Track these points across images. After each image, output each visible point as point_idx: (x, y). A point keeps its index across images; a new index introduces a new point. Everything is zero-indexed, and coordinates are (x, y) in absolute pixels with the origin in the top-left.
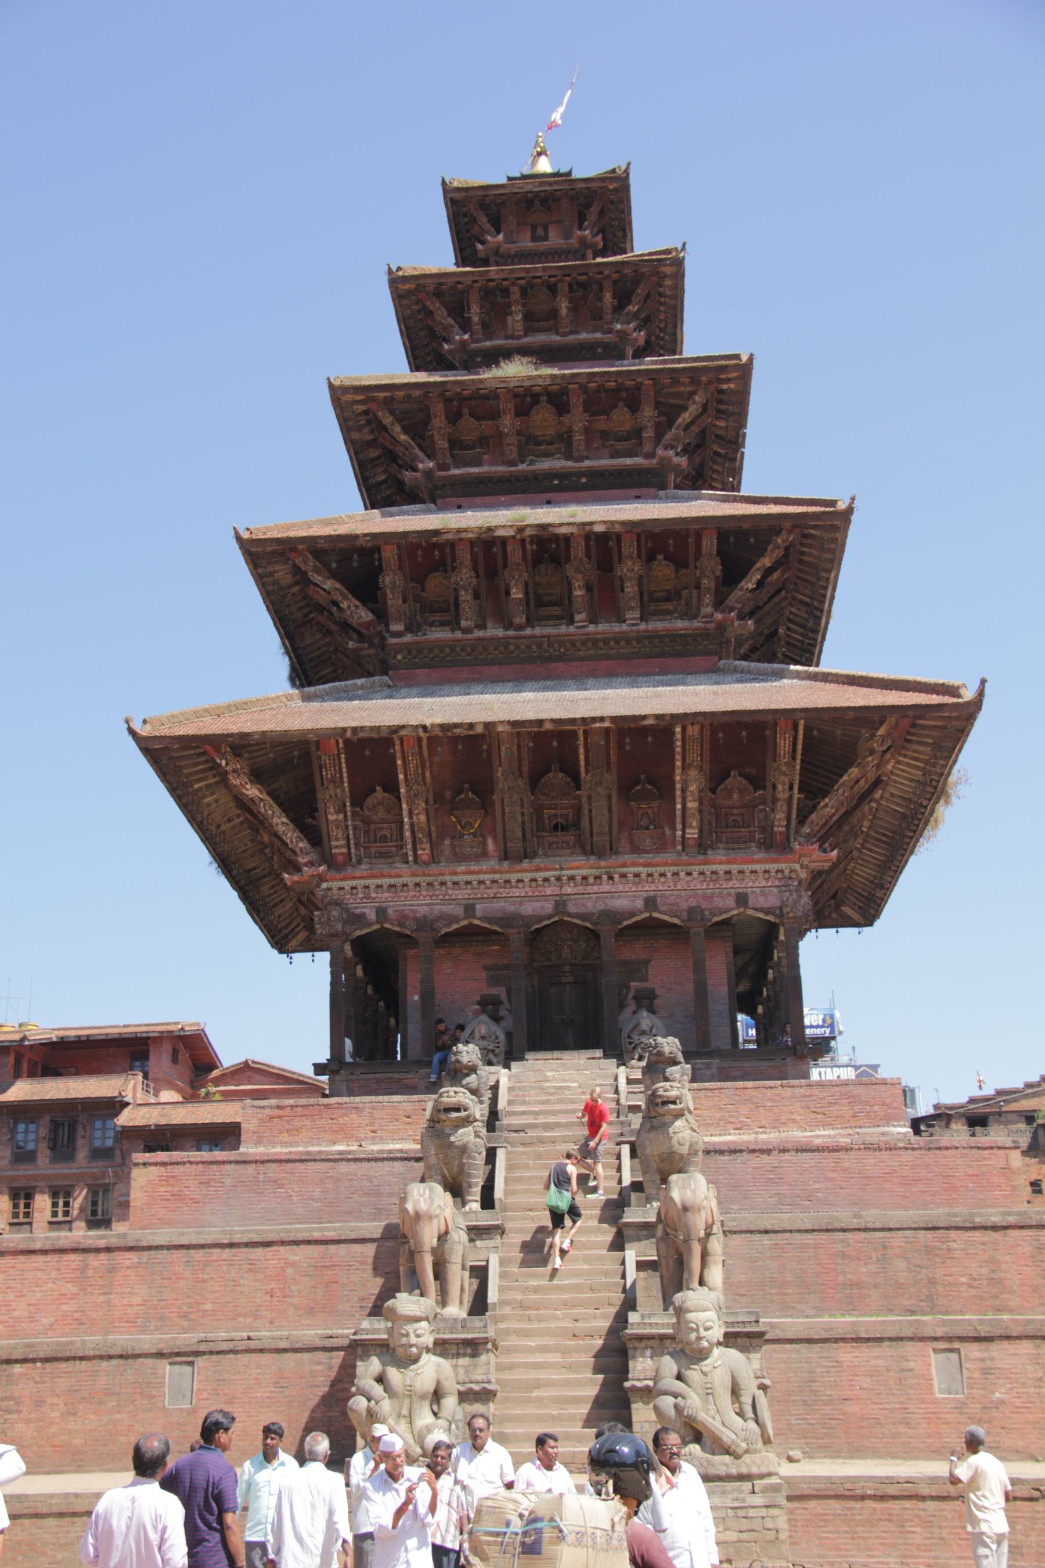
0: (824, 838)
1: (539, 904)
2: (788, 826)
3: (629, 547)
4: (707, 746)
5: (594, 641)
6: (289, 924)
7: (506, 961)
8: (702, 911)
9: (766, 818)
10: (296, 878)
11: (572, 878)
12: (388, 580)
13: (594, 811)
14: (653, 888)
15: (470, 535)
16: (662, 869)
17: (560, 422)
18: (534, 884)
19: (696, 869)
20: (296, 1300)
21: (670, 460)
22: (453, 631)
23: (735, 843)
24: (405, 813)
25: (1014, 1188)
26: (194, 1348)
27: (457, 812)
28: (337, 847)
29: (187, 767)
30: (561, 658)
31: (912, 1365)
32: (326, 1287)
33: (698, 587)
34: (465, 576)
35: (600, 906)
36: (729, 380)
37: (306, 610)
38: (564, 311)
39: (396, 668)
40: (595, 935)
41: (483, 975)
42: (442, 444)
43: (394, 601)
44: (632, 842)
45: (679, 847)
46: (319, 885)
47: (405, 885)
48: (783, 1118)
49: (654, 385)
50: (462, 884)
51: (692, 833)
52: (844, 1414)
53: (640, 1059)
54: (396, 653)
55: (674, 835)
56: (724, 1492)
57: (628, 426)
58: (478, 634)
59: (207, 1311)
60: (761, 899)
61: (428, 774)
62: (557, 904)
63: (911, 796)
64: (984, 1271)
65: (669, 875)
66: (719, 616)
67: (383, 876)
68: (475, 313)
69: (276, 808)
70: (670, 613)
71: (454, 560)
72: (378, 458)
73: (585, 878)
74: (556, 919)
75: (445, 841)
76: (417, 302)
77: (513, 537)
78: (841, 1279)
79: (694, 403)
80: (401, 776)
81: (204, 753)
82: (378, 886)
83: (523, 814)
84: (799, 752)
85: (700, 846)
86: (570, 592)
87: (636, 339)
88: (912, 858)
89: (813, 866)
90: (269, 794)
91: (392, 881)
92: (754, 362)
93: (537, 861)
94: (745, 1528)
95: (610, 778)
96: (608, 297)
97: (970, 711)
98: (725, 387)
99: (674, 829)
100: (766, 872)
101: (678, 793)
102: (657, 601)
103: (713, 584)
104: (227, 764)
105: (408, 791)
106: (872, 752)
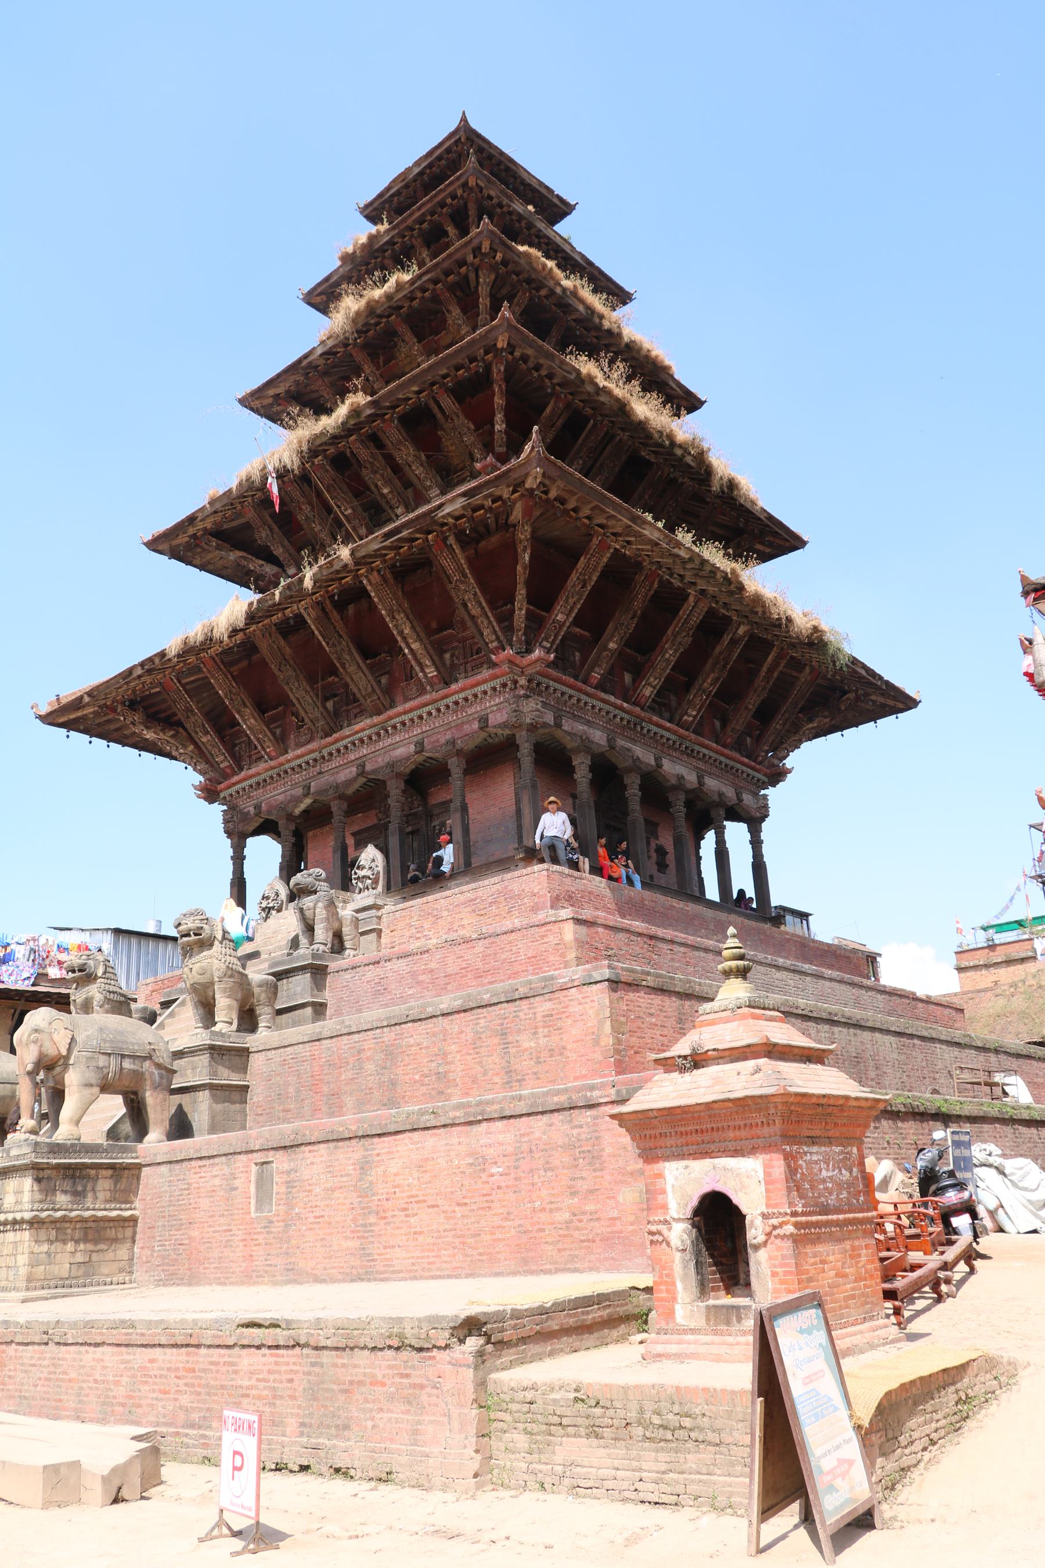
1: (347, 771)
2: (498, 638)
3: (393, 433)
12: (264, 536)
14: (419, 731)
19: (441, 705)
31: (237, 1183)
43: (278, 551)
44: (404, 695)
45: (428, 688)
47: (265, 780)
51: (431, 672)
52: (190, 1238)
60: (498, 716)
64: (434, 1064)
74: (362, 780)
78: (325, 1089)
82: (251, 786)
84: (465, 566)
89: (530, 671)
96: (451, 230)
100: (494, 689)
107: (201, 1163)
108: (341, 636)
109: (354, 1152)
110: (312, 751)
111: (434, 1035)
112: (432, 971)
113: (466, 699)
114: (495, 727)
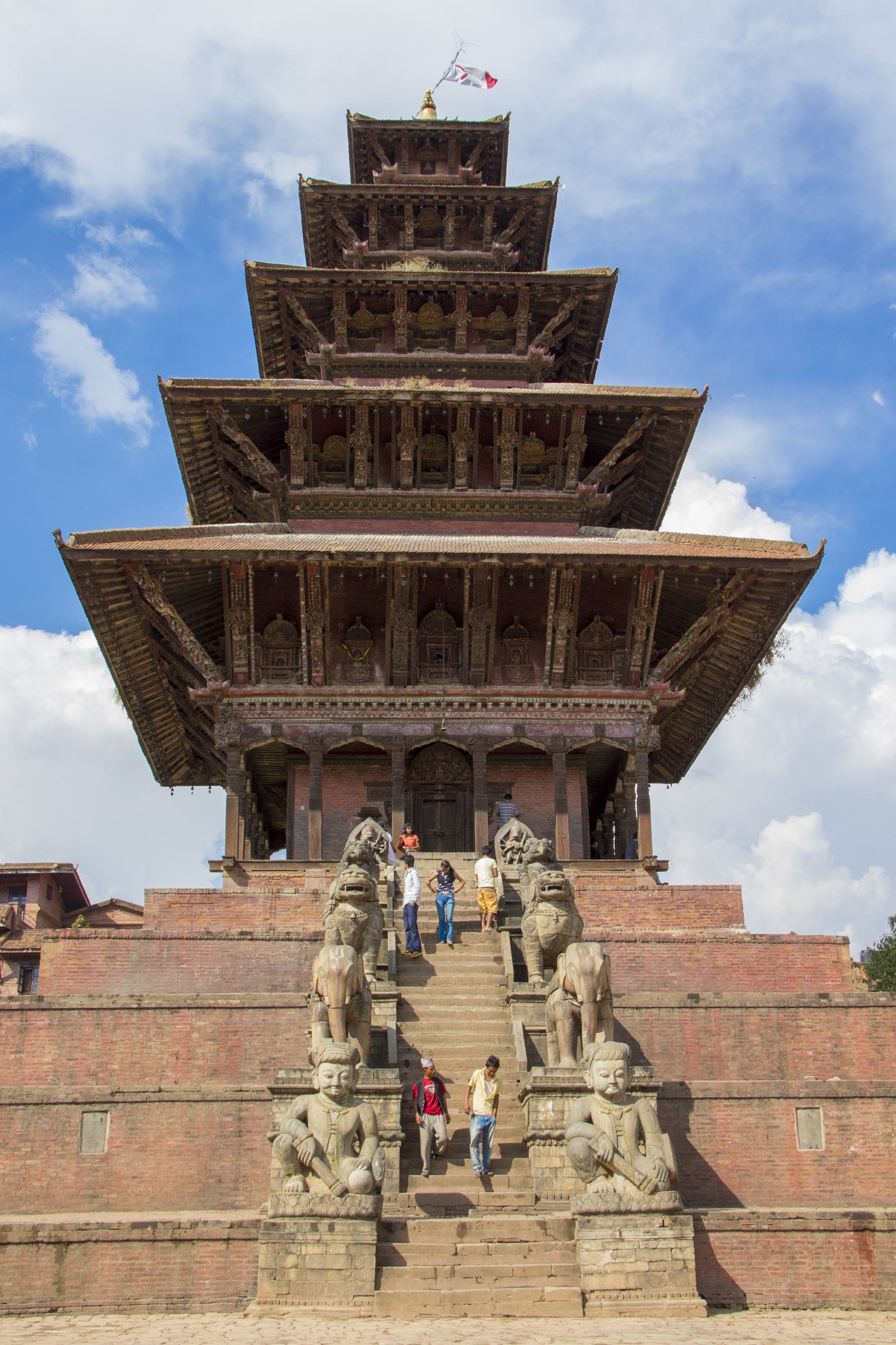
0: (675, 677)
1: (419, 726)
2: (642, 666)
3: (509, 419)
4: (578, 590)
5: (472, 504)
6: (174, 758)
7: (384, 779)
8: (565, 738)
9: (624, 660)
10: (200, 691)
11: (450, 704)
13: (473, 644)
14: (522, 716)
15: (372, 397)
16: (531, 700)
17: (444, 320)
18: (416, 708)
19: (560, 701)
20: (200, 1062)
21: (540, 356)
22: (347, 487)
23: (594, 679)
24: (303, 637)
25: (844, 979)
26: (110, 1098)
27: (349, 641)
28: (239, 666)
29: (105, 586)
30: (442, 517)
31: (778, 1122)
32: (229, 1051)
33: (565, 463)
34: (361, 438)
35: (476, 731)
36: (595, 292)
37: (212, 467)
38: (450, 229)
39: (295, 518)
40: (467, 756)
41: (364, 790)
42: (341, 330)
43: (296, 456)
44: (504, 676)
45: (546, 681)
46: (220, 700)
48: (639, 918)
49: (530, 290)
50: (351, 706)
51: (559, 669)
53: (511, 861)
54: (295, 504)
55: (543, 670)
56: (636, 1226)
57: (503, 328)
58: (368, 491)
59: (114, 1070)
60: (616, 730)
61: (327, 602)
62: (437, 727)
63: (739, 654)
64: (828, 1045)
65: (537, 705)
66: (582, 486)
67: (280, 694)
68: (373, 225)
69: (186, 627)
70: (538, 484)
71: (353, 421)
72: (281, 344)
73: (461, 704)
74: (434, 740)
75: (338, 667)
76: (322, 213)
77: (408, 402)
79: (563, 309)
80: (303, 603)
81: (121, 574)
82: (276, 704)
83: (410, 646)
84: (658, 600)
85: (564, 681)
86: (453, 460)
87: (511, 258)
88: (726, 717)
89: (663, 703)
90: (179, 613)
91: (288, 699)
92: (619, 275)
93: (419, 688)
94: (654, 1258)
95: (491, 616)
98: (591, 297)
99: (542, 665)
100: (622, 706)
101: (549, 631)
102: (529, 472)
103: (578, 460)
104: (144, 583)
105: (307, 617)
106: (720, 603)
107: (726, 1102)
108: (490, 606)
110: (380, 695)
111: (828, 1022)
112: (699, 960)
113: (588, 705)
114: (612, 739)
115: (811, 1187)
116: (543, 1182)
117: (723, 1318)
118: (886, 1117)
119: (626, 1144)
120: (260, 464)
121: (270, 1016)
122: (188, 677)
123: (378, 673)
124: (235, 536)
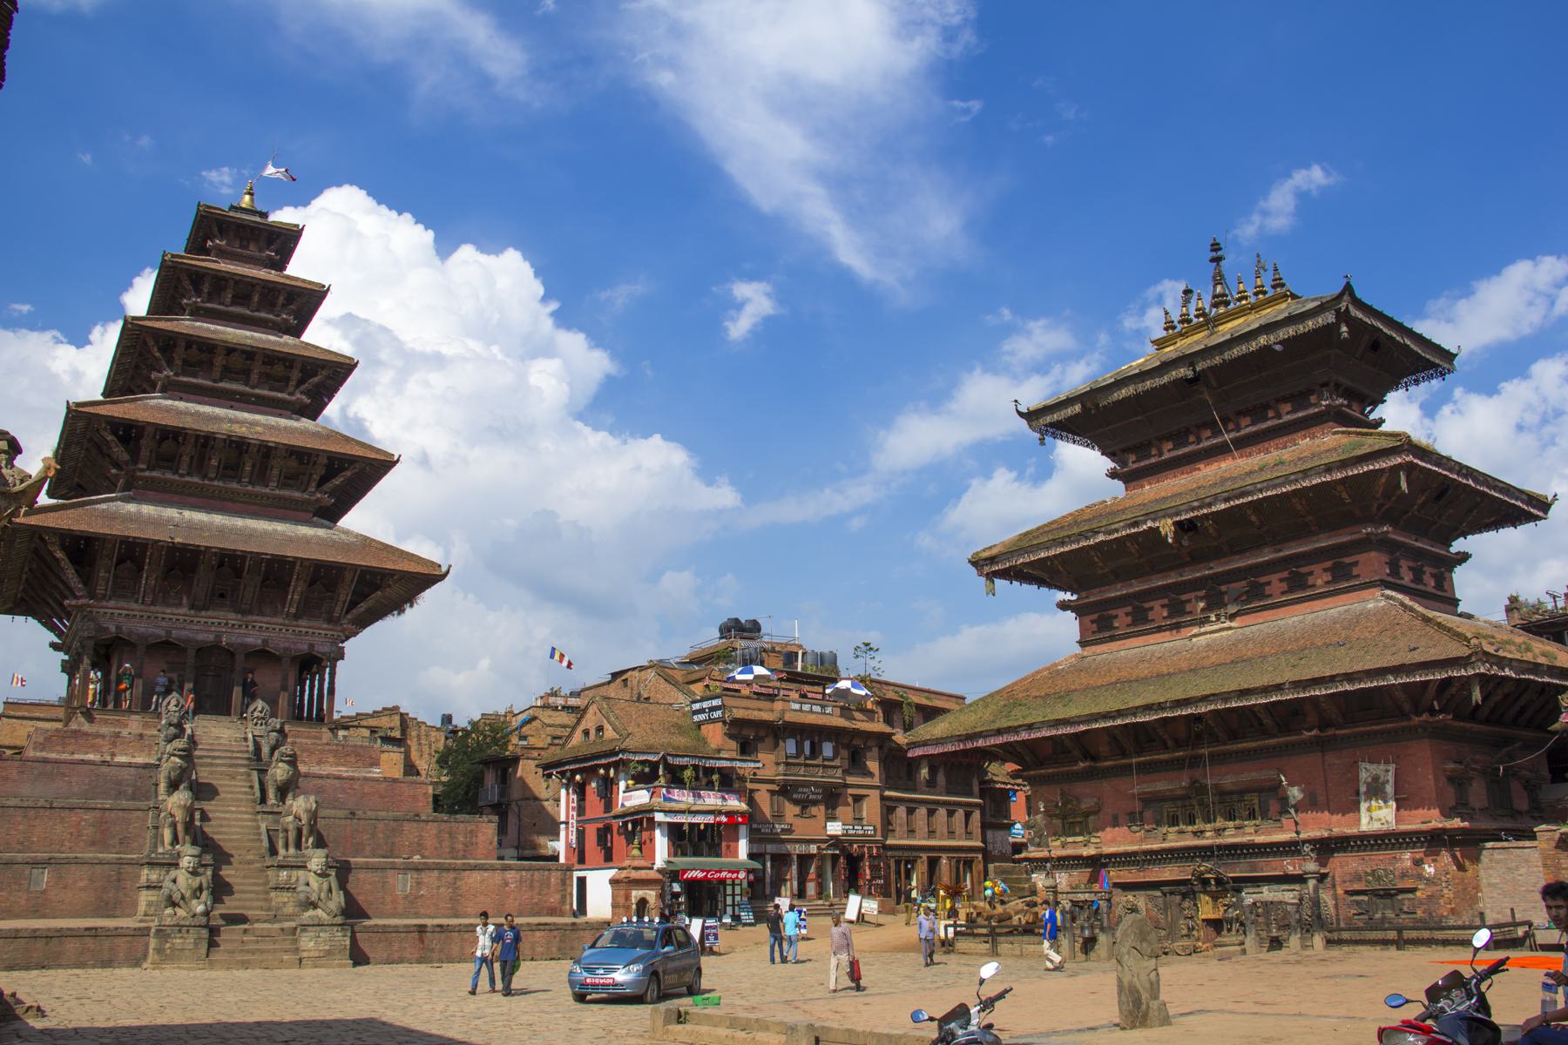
5: (250, 494)
30: (231, 500)
34: (188, 450)
40: (232, 654)
42: (178, 362)
51: (293, 610)
58: (188, 479)
68: (206, 288)
75: (162, 595)
93: (210, 613)
96: (281, 299)
97: (443, 577)
109: (452, 875)
115: (400, 909)
116: (278, 909)
117: (360, 969)
118: (439, 878)
119: (323, 895)
120: (120, 452)
121: (126, 815)
122: (67, 593)
123: (185, 600)
124: (104, 506)
